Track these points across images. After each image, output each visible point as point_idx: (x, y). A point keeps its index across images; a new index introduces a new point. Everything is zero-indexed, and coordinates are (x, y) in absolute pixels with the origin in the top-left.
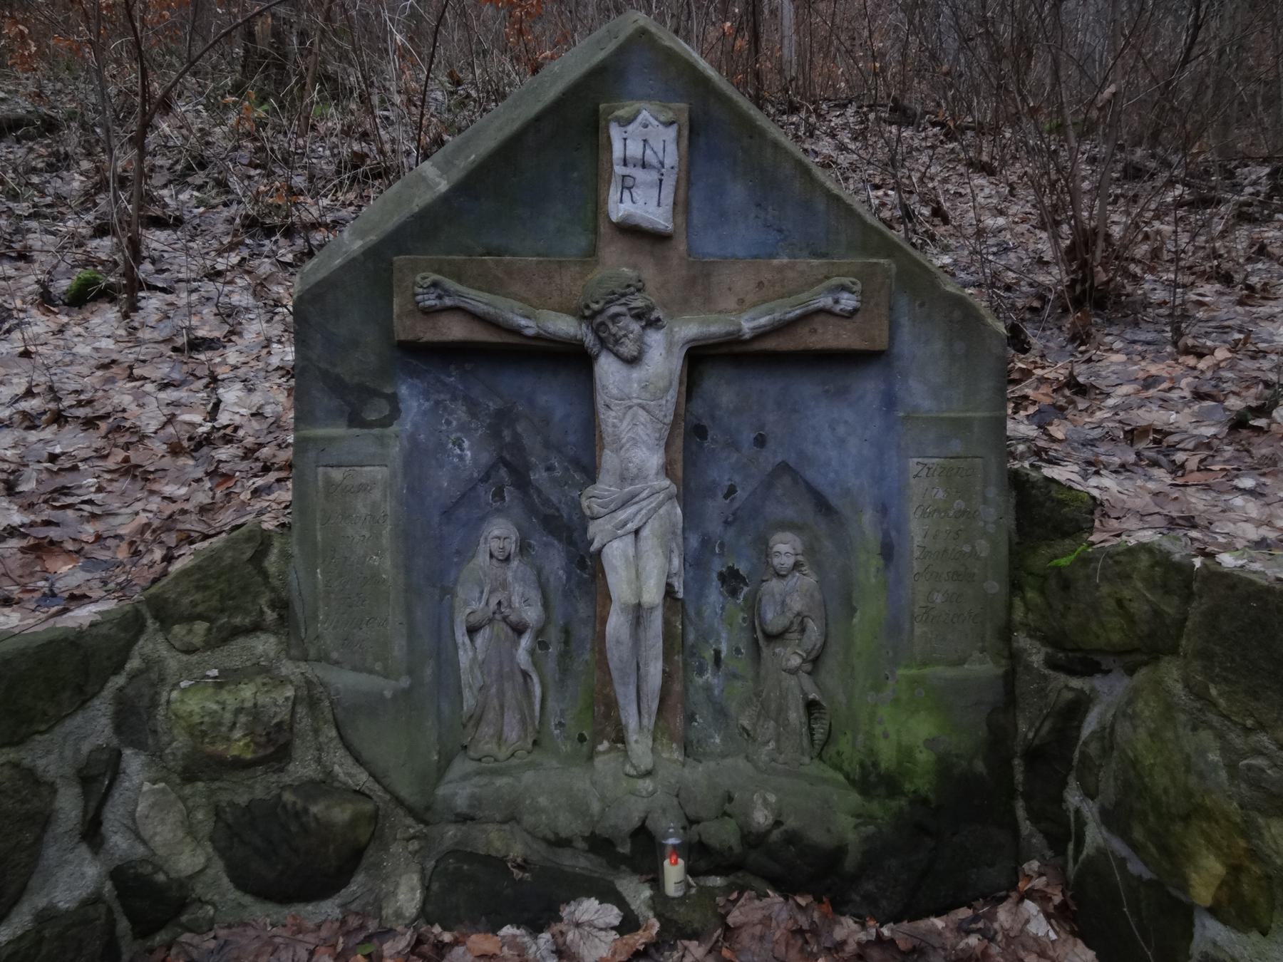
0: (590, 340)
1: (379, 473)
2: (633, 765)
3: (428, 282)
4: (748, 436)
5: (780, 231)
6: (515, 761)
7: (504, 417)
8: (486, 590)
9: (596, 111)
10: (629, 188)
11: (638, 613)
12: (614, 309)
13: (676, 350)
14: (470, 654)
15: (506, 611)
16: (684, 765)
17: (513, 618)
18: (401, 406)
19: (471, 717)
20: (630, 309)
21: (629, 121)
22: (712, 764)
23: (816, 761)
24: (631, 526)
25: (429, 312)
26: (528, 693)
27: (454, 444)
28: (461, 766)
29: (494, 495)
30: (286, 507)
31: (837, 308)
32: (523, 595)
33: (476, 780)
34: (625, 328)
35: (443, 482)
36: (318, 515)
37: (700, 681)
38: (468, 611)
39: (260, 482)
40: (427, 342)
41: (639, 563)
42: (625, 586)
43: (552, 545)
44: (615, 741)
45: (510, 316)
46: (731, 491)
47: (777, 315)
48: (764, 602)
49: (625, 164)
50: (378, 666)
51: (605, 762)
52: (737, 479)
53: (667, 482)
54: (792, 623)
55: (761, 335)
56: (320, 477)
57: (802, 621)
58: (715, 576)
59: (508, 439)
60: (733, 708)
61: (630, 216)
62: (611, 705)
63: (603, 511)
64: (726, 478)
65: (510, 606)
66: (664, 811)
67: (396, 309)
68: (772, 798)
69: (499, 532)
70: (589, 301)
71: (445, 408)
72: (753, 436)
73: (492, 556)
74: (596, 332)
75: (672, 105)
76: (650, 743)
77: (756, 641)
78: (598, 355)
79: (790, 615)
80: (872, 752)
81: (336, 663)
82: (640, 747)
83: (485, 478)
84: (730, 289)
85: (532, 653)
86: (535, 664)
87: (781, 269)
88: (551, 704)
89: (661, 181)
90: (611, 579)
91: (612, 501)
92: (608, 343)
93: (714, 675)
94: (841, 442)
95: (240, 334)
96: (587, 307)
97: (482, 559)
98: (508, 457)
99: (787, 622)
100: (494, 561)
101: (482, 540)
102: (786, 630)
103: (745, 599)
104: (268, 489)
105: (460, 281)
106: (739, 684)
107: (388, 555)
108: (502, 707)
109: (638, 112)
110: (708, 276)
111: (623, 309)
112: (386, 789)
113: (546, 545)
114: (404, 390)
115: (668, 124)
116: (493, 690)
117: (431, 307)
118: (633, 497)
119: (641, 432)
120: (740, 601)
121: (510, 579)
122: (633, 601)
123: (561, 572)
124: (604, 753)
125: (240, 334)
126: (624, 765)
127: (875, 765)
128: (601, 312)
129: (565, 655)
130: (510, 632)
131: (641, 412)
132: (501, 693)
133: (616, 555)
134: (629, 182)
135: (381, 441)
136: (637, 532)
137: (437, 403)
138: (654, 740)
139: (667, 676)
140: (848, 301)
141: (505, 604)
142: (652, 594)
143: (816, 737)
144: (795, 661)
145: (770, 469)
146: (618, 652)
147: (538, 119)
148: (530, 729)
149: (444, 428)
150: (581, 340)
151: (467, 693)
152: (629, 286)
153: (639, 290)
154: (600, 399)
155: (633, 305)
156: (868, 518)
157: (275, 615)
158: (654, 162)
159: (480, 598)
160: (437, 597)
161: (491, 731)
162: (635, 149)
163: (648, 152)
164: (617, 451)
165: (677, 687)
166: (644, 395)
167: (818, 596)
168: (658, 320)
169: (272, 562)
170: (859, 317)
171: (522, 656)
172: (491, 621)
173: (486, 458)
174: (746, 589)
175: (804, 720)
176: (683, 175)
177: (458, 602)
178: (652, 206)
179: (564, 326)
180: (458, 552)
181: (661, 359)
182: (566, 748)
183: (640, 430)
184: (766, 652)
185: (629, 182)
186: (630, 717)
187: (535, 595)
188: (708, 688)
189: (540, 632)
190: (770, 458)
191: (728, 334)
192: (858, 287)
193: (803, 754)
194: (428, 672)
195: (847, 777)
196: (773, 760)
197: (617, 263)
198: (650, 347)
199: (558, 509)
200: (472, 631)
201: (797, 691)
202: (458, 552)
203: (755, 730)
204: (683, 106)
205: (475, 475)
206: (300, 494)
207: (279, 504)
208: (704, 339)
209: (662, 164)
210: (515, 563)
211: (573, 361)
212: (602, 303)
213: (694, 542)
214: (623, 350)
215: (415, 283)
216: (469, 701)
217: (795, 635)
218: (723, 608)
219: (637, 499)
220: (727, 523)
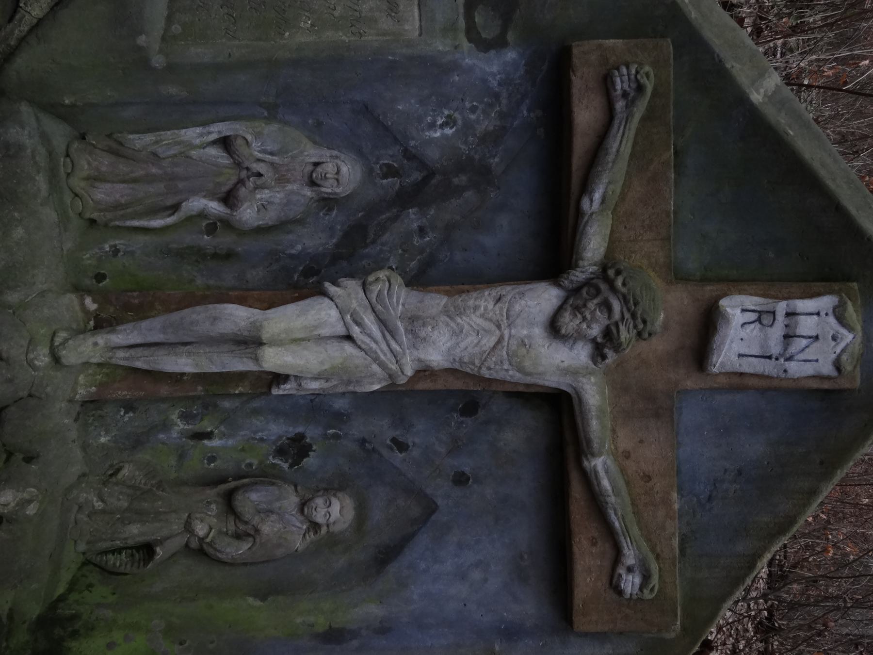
0: (578, 276)
1: (412, 25)
2: (66, 340)
3: (644, 80)
4: (466, 464)
5: (710, 499)
6: (68, 198)
7: (482, 176)
8: (275, 159)
9: (848, 279)
10: (759, 320)
11: (250, 342)
12: (616, 306)
13: (568, 380)
14: (197, 142)
15: (250, 184)
16: (71, 401)
17: (243, 192)
18: (492, 53)
19: (121, 144)
20: (617, 325)
21: (841, 319)
22: (73, 434)
23: (81, 558)
24: (356, 331)
25: (606, 82)
26: (154, 211)
27: (449, 116)
28: (59, 133)
29: (388, 166)
31: (622, 571)
33: (42, 150)
34: (594, 319)
35: (404, 104)
37: (174, 417)
38: (249, 138)
40: (570, 81)
41: (310, 341)
42: (283, 325)
44: (97, 317)
45: (605, 180)
46: (402, 446)
47: (612, 499)
48: (271, 488)
49: (788, 315)
50: (176, 28)
51: (70, 306)
52: (415, 453)
53: (409, 372)
54: (246, 523)
55: (588, 480)
57: (249, 535)
58: (300, 429)
59: (456, 181)
60: (144, 456)
61: (727, 320)
62: (139, 311)
63: (373, 297)
64: (417, 440)
65: (257, 187)
66: (10, 381)
67: (610, 42)
68: (31, 510)
69: (345, 173)
70: (625, 274)
71: (491, 105)
72: (467, 470)
73: (316, 164)
74: (588, 283)
75: (858, 369)
76: (94, 360)
77: (224, 481)
78: (559, 286)
79: (256, 520)
80: (91, 628)
82: (90, 349)
83: (409, 155)
84: (641, 442)
85: (202, 215)
86: (190, 219)
87: (666, 502)
88: (142, 239)
89: (770, 357)
90: (291, 309)
91: (385, 307)
92: (575, 299)
93: (182, 433)
94: (462, 576)
96: (618, 273)
97: (312, 153)
98: (434, 181)
99: (247, 517)
100: (310, 168)
101: (335, 153)
102: (237, 516)
103: (274, 465)
105: (644, 119)
106: (173, 461)
107: (312, 38)
108: (135, 181)
109: (850, 329)
110: (657, 415)
111: (617, 315)
112: (22, 40)
114: (511, 55)
115: (837, 365)
116: (154, 170)
117: (613, 84)
118: (390, 332)
119: (469, 339)
120: (272, 460)
121: (290, 187)
122: (265, 337)
123: (299, 247)
124: (82, 304)
126: (66, 329)
127: (75, 634)
128: (613, 289)
129: (199, 255)
131: (493, 340)
132: (150, 179)
133: (321, 314)
134: (767, 320)
135: (450, 29)
136: (349, 338)
137: (497, 96)
138: (99, 365)
139: (177, 378)
140: (630, 583)
141: (260, 182)
142: (273, 359)
143: (110, 556)
144: (200, 529)
145: (429, 491)
146: (199, 318)
147: (839, 209)
148: (109, 215)
149: (468, 105)
150: (577, 266)
151: (149, 138)
152: (644, 322)
153: (639, 334)
154: (507, 290)
155: (622, 328)
156: (373, 610)
158: (793, 349)
159: (264, 152)
160: (263, 99)
161: (104, 169)
162: (807, 326)
163: (804, 342)
164: (446, 312)
165: (164, 390)
166: (514, 343)
167: (280, 552)
168: (604, 357)
170: (611, 595)
171: (197, 204)
173: (433, 154)
174: (285, 466)
175: (130, 542)
176: (776, 383)
178: (738, 347)
179: (594, 245)
180: (319, 124)
181: (558, 361)
182: (88, 258)
183: (472, 339)
184: (211, 493)
185: (767, 320)
186: (125, 335)
187: (270, 217)
188: (166, 426)
189: (227, 224)
190: (441, 491)
191: (589, 442)
192: (647, 595)
193: (88, 543)
194: (172, 90)
195: (62, 598)
196: (80, 507)
197: (670, 306)
198: (571, 348)
199: (374, 242)
200: (225, 143)
201: (165, 532)
202: (319, 124)
203: (117, 484)
204: (858, 382)
205: (412, 143)
208: (581, 412)
209: (790, 359)
210: (308, 192)
211: (550, 255)
212: (624, 290)
213: (340, 404)
214: (567, 316)
215: (641, 65)
216: (140, 141)
217: (232, 528)
218: (262, 440)
219: (389, 337)
220: (363, 442)
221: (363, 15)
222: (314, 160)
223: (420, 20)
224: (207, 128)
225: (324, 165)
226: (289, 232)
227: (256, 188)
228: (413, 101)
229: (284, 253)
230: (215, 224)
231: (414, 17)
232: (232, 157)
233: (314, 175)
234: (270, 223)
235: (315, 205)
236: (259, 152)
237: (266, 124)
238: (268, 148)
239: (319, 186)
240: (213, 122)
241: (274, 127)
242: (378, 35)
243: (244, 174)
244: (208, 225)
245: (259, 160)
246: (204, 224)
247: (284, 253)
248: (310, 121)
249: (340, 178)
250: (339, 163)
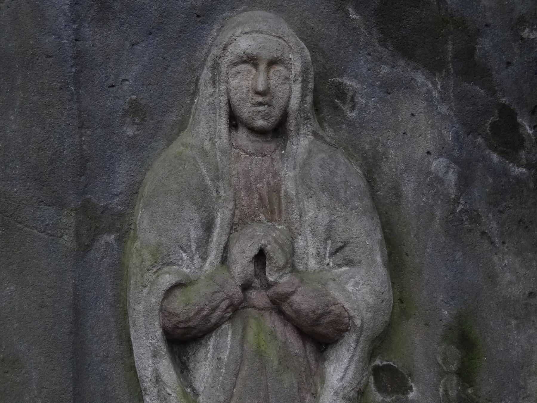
8: (221, 219)
15: (284, 281)
17: (303, 301)
32: (330, 230)
38: (167, 279)
43: (409, 86)
65: (291, 266)
73: (234, 121)
97: (208, 128)
100: (243, 137)
101: (206, 74)
113: (388, 87)
121: (289, 186)
123: (438, 165)
130: (295, 344)
141: (277, 257)
159: (204, 244)
160: (68, 240)
172: (236, 309)
177: (138, 254)
180: (136, 110)
187: (363, 231)
189: (380, 342)
200: (182, 341)
202: (136, 110)
210: (301, 143)
222: (223, 125)
224: (147, 384)
225: (235, 98)
226: (397, 191)
227: (294, 270)
229: (456, 201)
230: (377, 371)
232: (217, 325)
233: (260, 123)
234: (379, 236)
235: (329, 132)
236: (204, 259)
237: (135, 238)
238: (193, 234)
239: (285, 115)
240: (133, 368)
241: (142, 219)
243: (258, 297)
244: (380, 388)
245: (224, 260)
246: (379, 397)
247: (456, 201)
248: (130, 132)
249: (266, 55)
250: (229, 58)
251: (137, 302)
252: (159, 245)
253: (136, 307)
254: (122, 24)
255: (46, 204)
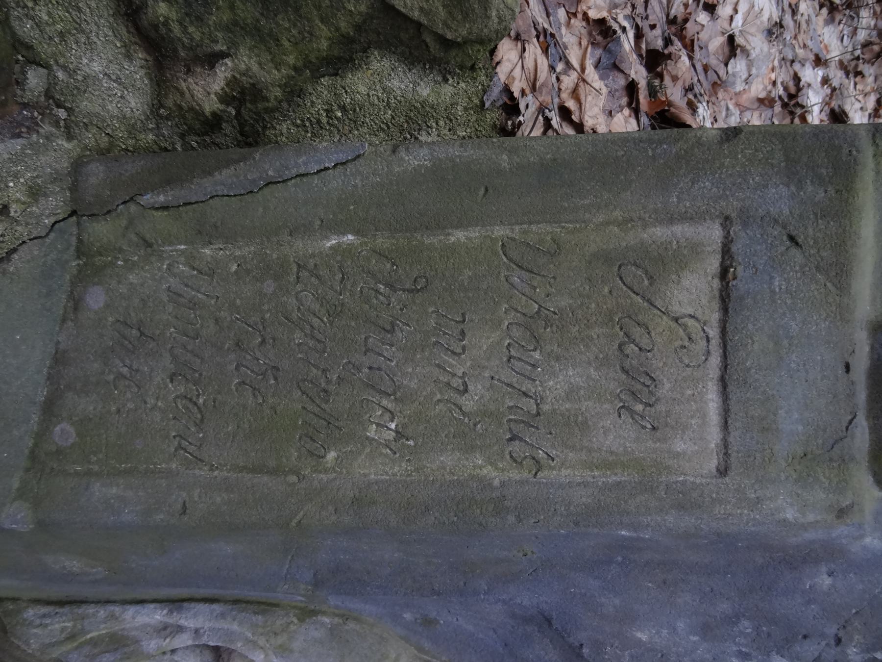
30: (565, 113)
36: (542, 231)
39: (627, 42)
50: (64, 433)
56: (682, 230)
81: (76, 304)
95: (830, 20)
104: (612, 65)
125: (830, 20)
157: (211, 105)
169: (382, 81)
202: (428, 622)
206: (609, 161)
207: (575, 93)
221: (546, 407)
223: (725, 426)
228: (681, 625)
231: (704, 416)
242: (590, 466)
251: (240, 624)
252: (292, 651)
253: (236, 622)
254: (513, 627)
255: (314, 575)
